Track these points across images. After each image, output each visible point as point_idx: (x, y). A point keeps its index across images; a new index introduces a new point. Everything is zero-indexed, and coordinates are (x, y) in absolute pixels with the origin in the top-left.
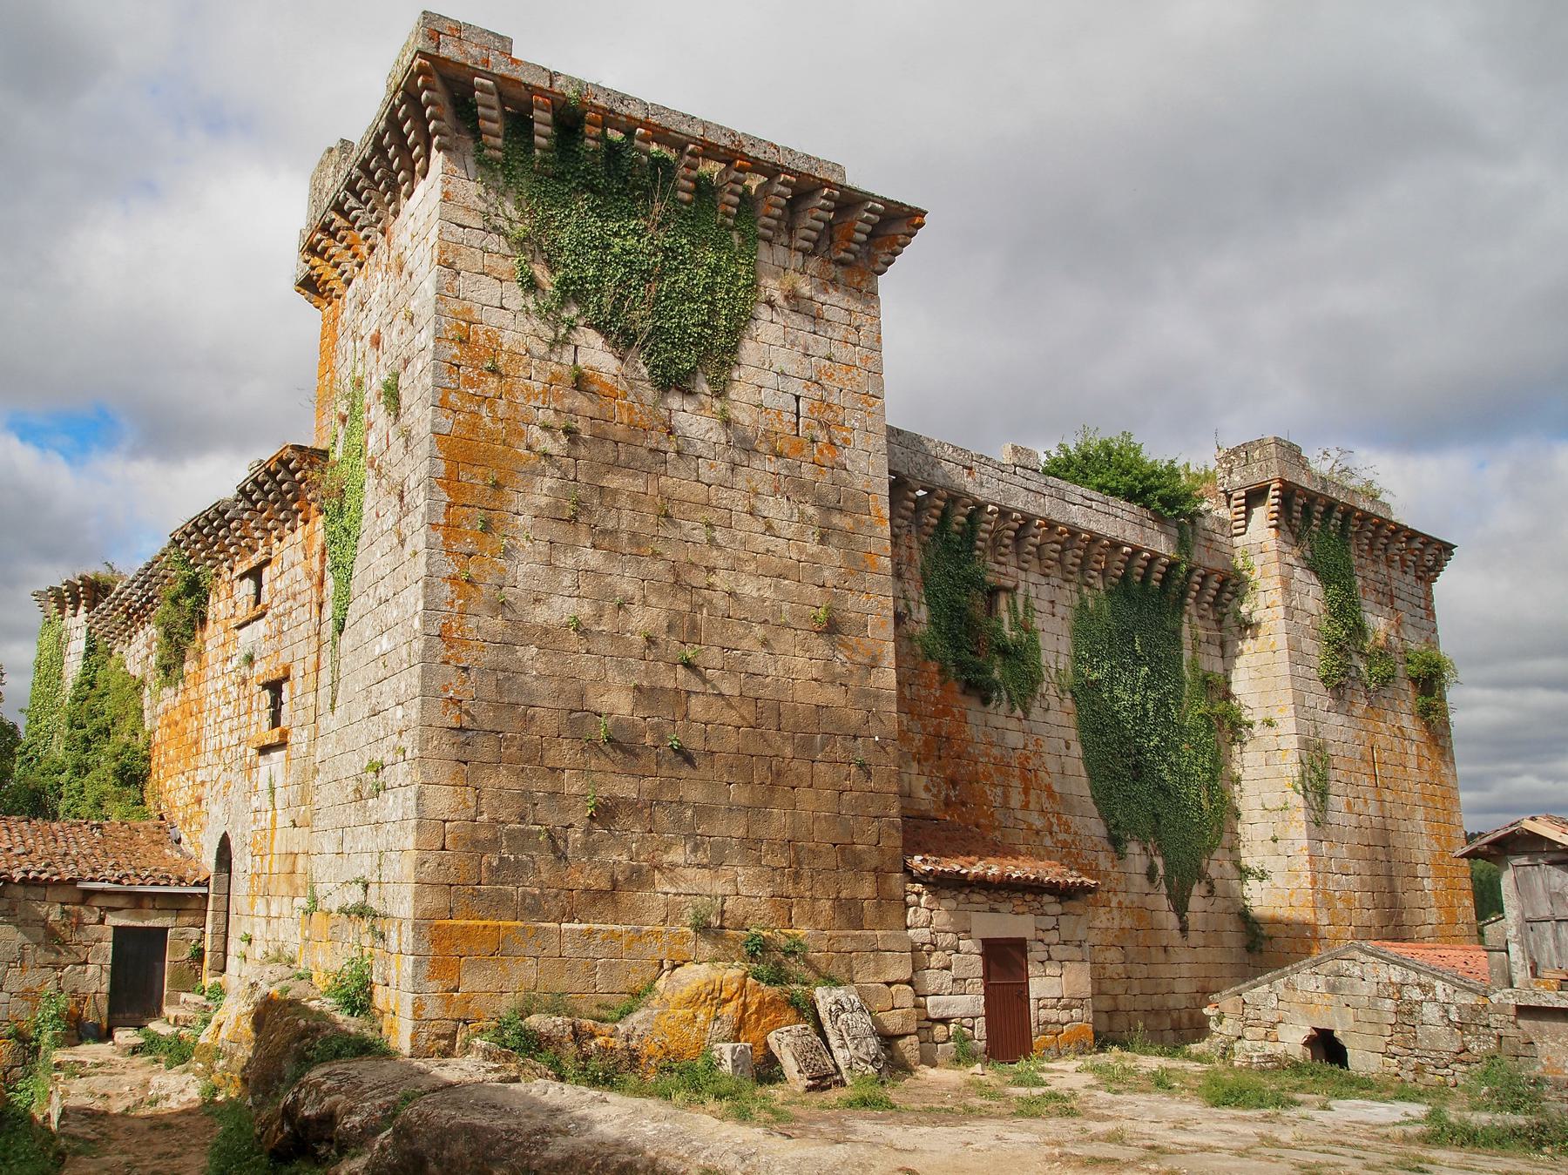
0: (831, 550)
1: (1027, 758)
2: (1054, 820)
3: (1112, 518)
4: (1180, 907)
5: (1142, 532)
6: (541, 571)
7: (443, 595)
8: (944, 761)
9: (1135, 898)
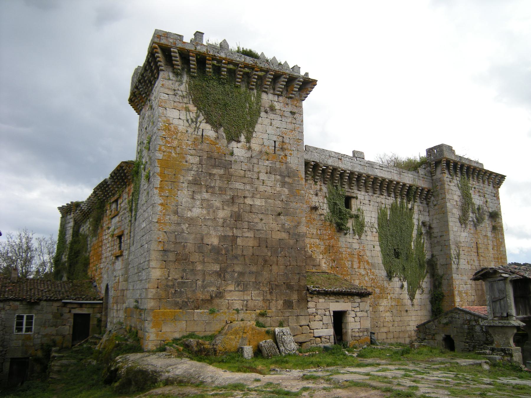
0: (285, 189)
1: (360, 252)
2: (369, 272)
3: (390, 173)
4: (412, 297)
5: (400, 176)
6: (189, 200)
8: (330, 254)
9: (396, 295)
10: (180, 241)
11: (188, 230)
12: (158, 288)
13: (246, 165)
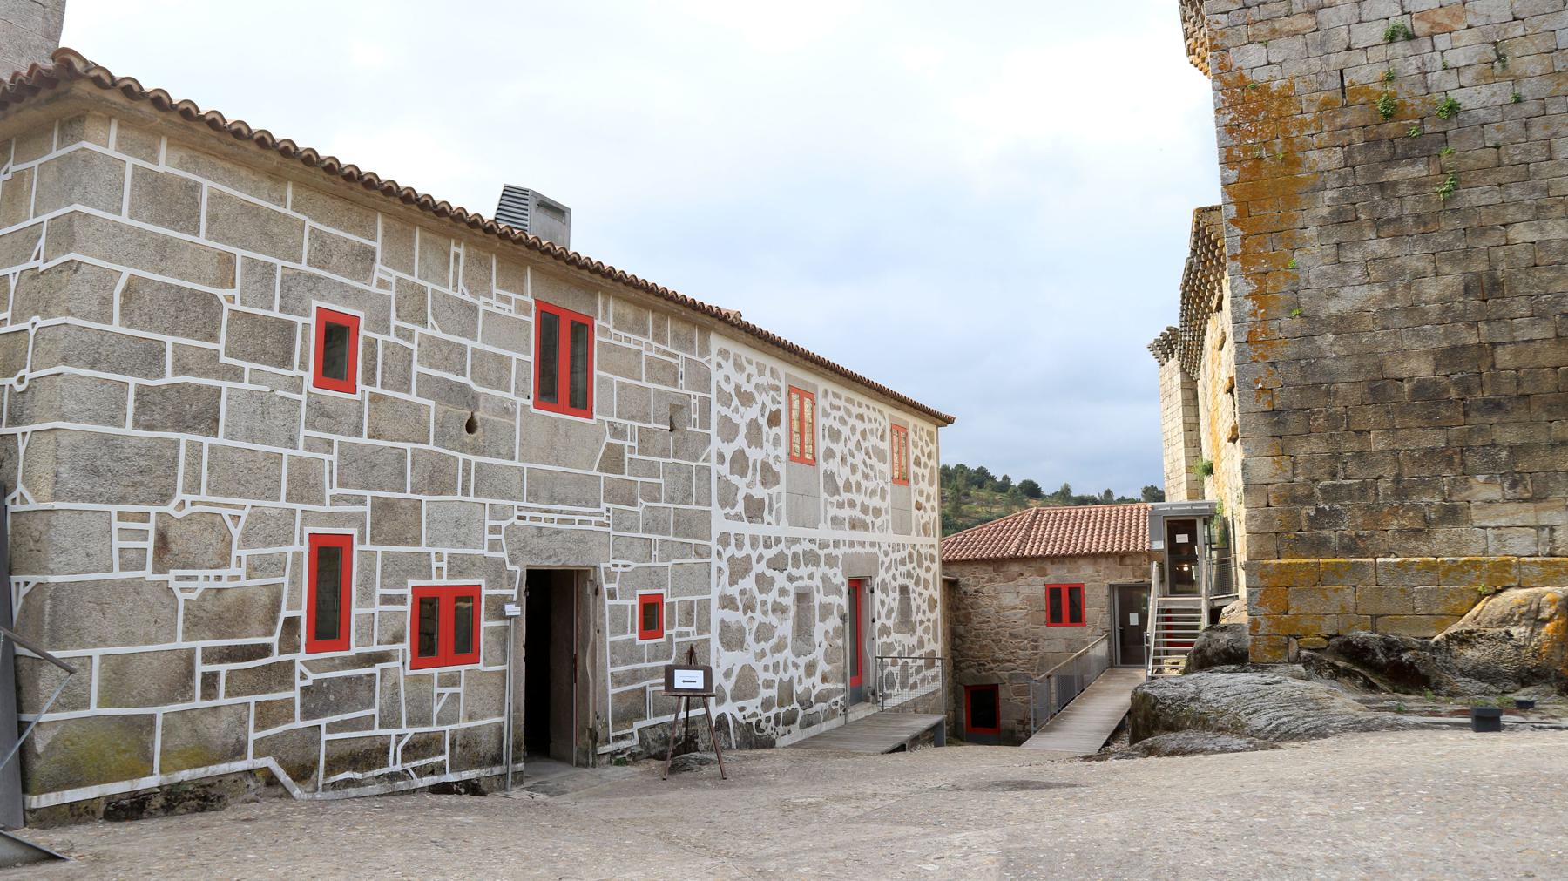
7: (1247, 309)
11: (1336, 348)
12: (1268, 506)
13: (1498, 129)
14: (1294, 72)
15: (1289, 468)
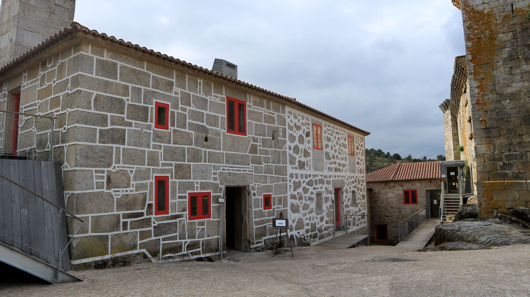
7: (476, 92)
10: (502, 117)
11: (510, 105)
14: (493, 6)
15: (492, 148)
